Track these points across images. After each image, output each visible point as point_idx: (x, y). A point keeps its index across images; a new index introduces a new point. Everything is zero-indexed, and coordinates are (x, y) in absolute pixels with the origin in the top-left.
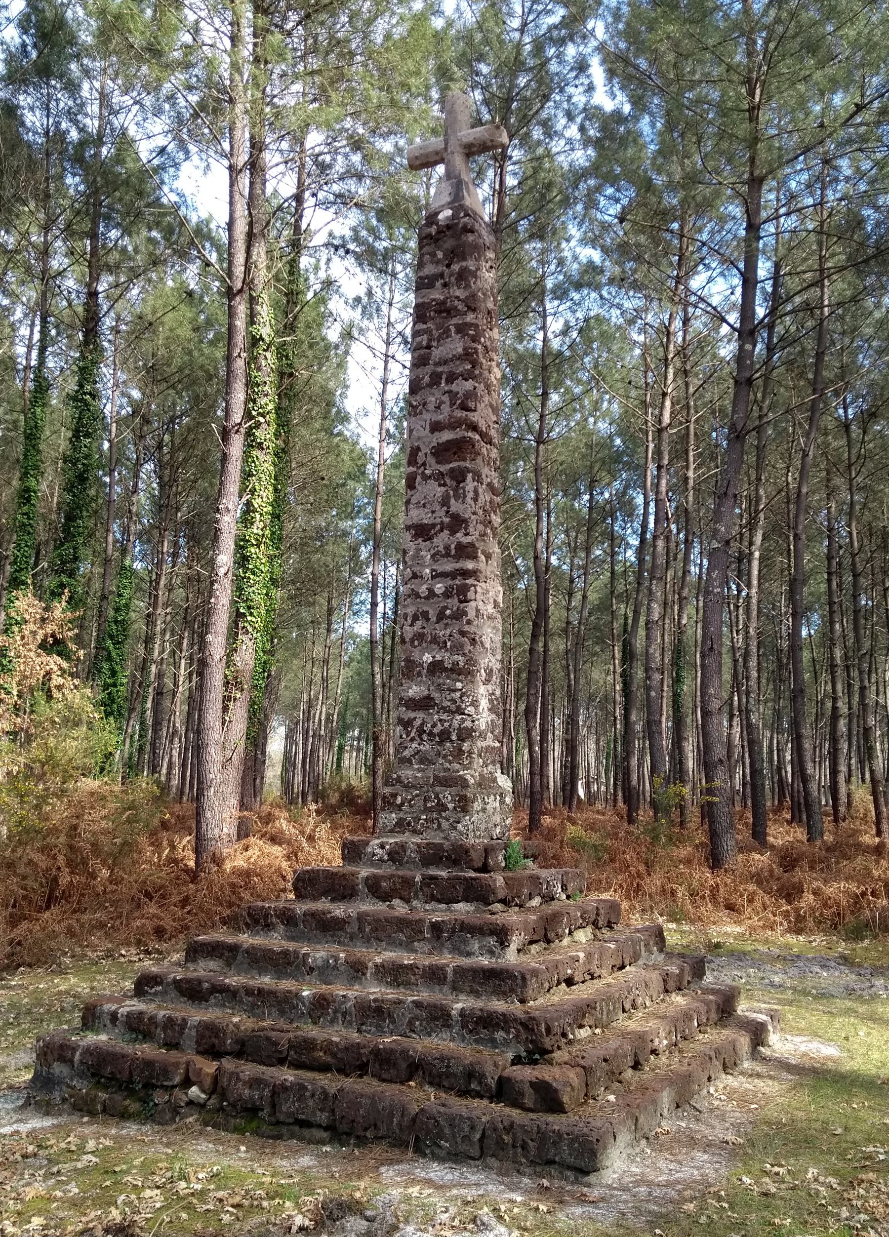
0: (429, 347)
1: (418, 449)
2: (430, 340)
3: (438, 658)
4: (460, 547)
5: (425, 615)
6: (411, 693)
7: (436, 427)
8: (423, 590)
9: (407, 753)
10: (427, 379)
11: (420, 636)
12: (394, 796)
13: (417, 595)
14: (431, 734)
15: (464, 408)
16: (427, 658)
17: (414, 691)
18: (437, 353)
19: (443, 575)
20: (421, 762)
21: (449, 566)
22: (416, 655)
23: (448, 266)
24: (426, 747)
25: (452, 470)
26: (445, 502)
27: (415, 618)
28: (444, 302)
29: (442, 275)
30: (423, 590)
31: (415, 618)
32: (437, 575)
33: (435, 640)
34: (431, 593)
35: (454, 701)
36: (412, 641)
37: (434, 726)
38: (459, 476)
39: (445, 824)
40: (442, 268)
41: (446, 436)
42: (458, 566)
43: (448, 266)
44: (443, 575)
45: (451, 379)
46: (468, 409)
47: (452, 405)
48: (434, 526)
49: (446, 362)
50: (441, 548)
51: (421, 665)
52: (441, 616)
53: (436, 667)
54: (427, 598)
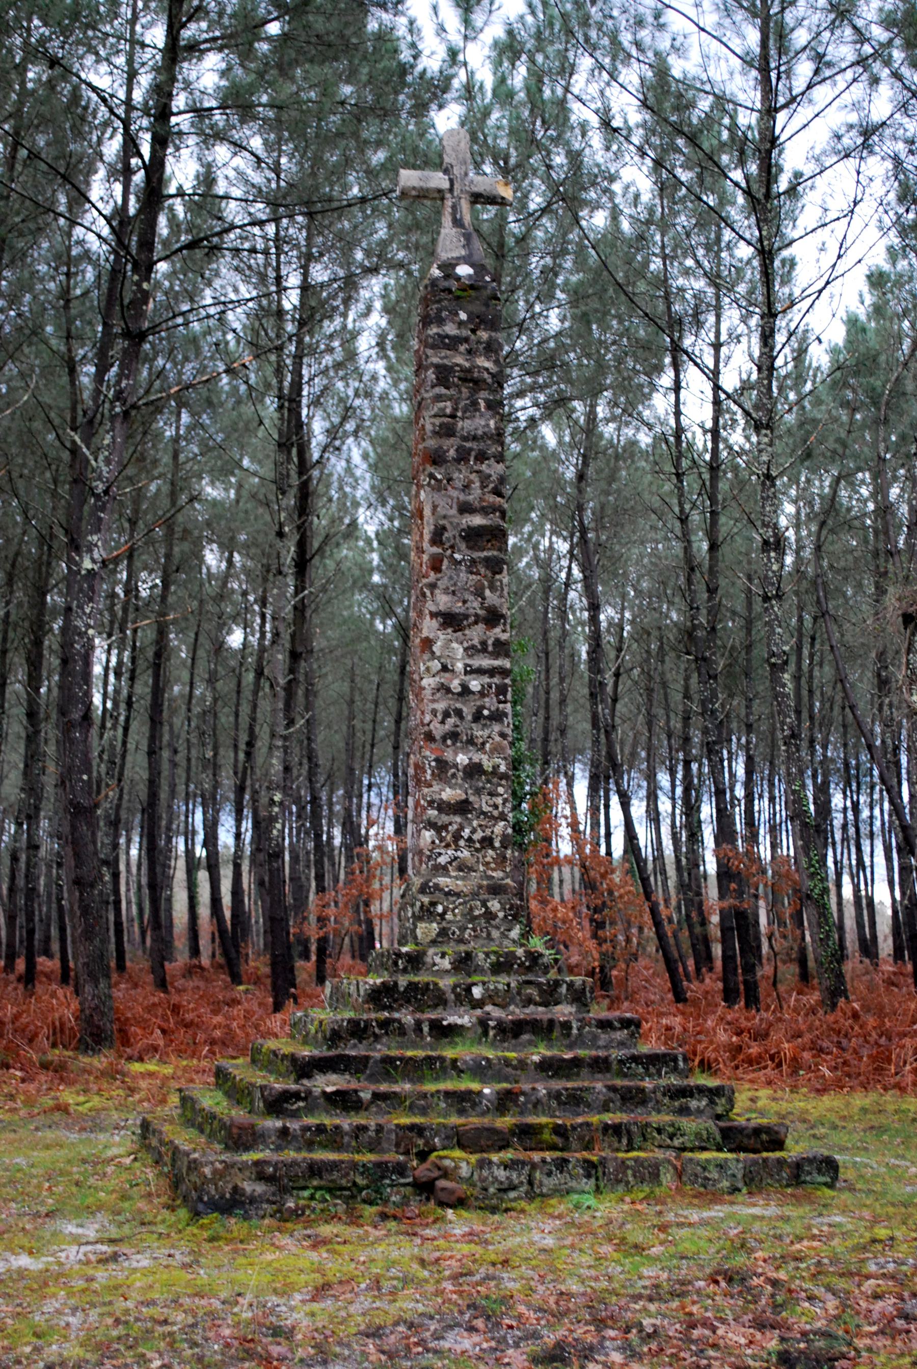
0: (453, 416)
1: (444, 528)
3: (476, 759)
5: (459, 713)
7: (465, 509)
9: (442, 860)
10: (452, 453)
11: (454, 735)
12: (433, 904)
13: (448, 690)
14: (470, 840)
16: (462, 759)
17: (449, 794)
18: (465, 425)
20: (460, 869)
21: (486, 662)
22: (448, 755)
23: (474, 331)
24: (465, 854)
25: (487, 560)
26: (479, 593)
27: (446, 715)
28: (469, 371)
30: (455, 685)
31: (446, 715)
32: (470, 671)
33: (471, 741)
34: (466, 690)
36: (444, 739)
37: (474, 831)
38: (495, 566)
39: (495, 934)
41: (477, 520)
43: (474, 331)
45: (482, 457)
47: (483, 487)
48: (466, 617)
49: (475, 438)
50: (476, 642)
52: (478, 717)
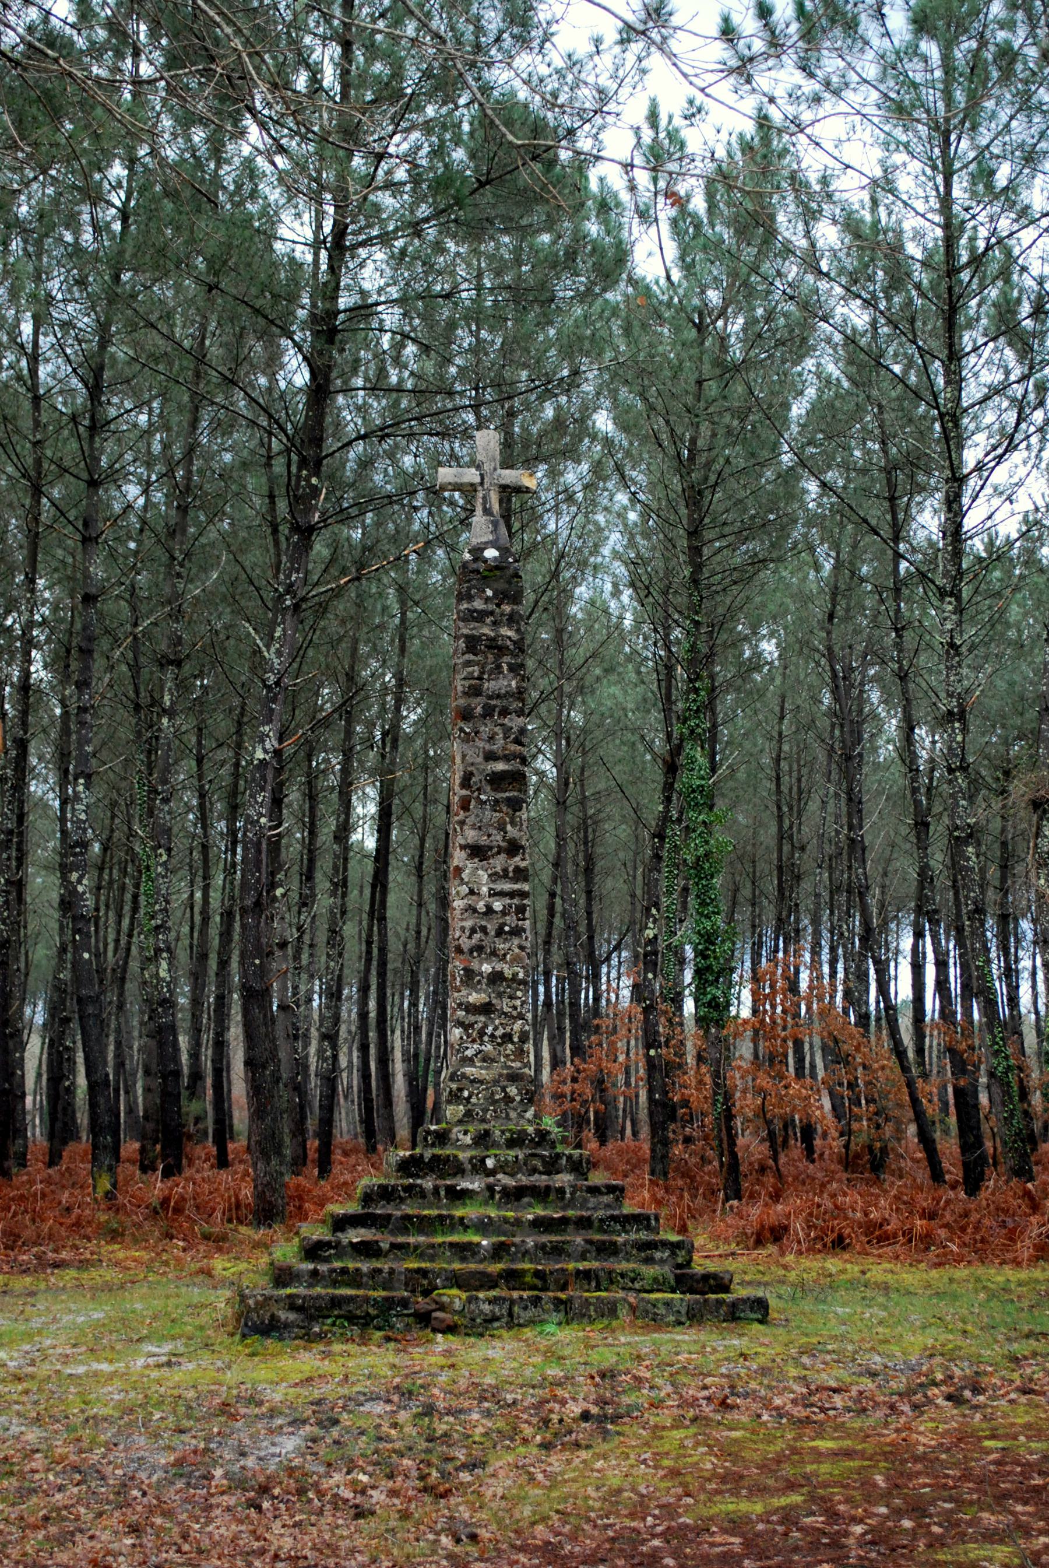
0: (480, 678)
2: (482, 673)
4: (517, 869)
5: (484, 930)
6: (471, 999)
7: (490, 757)
8: (481, 906)
11: (480, 948)
12: (461, 1090)
13: (475, 911)
14: (492, 1036)
15: (518, 742)
16: (486, 968)
18: (490, 686)
19: (501, 894)
20: (484, 1060)
22: (475, 965)
23: (498, 605)
24: (488, 1047)
25: (508, 799)
26: (502, 828)
27: (473, 931)
28: (494, 639)
29: (492, 613)
30: (481, 906)
31: (473, 931)
32: (494, 894)
34: (489, 910)
35: (515, 1008)
37: (496, 1029)
38: (516, 805)
40: (491, 607)
41: (500, 766)
42: (516, 887)
43: (498, 605)
44: (501, 894)
45: (505, 712)
46: (521, 744)
47: (505, 738)
48: (491, 848)
49: (499, 696)
50: (499, 869)
51: (481, 974)
52: (500, 932)
53: (496, 978)
54: (485, 914)
